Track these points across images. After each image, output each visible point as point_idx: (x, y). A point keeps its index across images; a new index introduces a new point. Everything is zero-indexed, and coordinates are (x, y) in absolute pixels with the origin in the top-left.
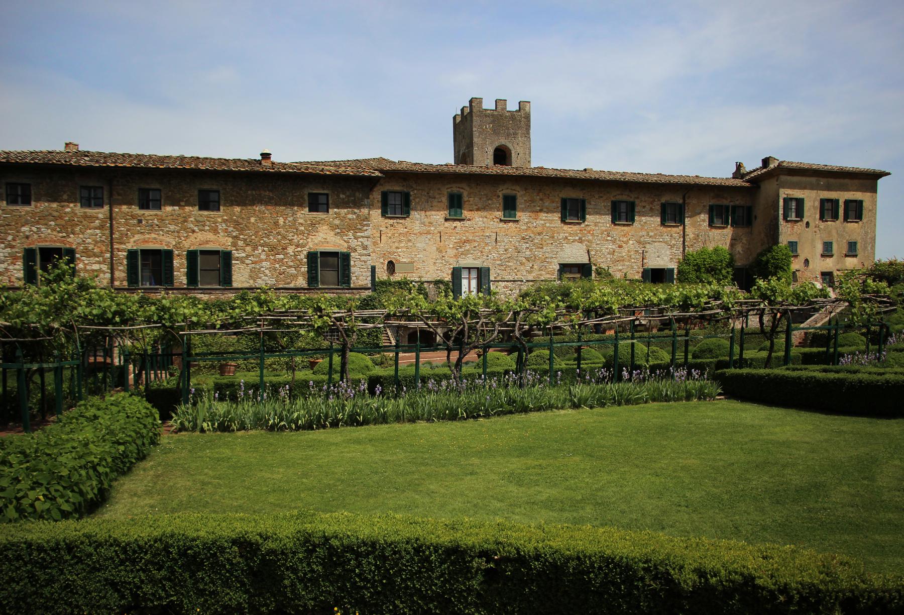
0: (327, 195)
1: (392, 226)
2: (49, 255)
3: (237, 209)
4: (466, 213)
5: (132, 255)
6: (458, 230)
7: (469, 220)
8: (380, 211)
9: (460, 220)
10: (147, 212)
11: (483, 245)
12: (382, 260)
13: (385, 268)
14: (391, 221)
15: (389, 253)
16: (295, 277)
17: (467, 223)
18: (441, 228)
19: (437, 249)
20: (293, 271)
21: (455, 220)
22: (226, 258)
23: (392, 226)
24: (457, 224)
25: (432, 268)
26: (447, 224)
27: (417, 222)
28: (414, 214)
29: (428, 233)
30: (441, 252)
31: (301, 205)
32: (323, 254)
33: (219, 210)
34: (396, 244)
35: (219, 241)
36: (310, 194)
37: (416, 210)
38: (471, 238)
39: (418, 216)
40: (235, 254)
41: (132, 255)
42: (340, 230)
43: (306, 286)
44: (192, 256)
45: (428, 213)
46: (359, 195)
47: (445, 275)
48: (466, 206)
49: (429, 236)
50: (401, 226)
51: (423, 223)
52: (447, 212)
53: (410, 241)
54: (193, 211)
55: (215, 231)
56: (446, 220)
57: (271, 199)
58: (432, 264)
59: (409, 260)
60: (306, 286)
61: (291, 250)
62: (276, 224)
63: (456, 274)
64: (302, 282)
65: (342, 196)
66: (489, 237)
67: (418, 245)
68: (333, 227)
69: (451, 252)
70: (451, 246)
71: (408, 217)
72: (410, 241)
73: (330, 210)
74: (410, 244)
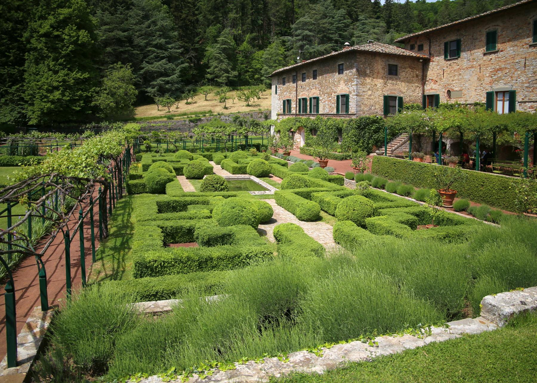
0: (343, 64)
1: (450, 65)
2: (288, 100)
3: (321, 77)
4: (499, 46)
5: (300, 100)
6: (492, 62)
7: (502, 51)
8: (443, 57)
9: (495, 53)
10: (304, 83)
11: (513, 70)
12: (444, 90)
13: (446, 95)
14: (449, 62)
15: (448, 85)
16: (333, 108)
17: (500, 54)
18: (481, 62)
19: (478, 78)
20: (333, 105)
21: (491, 53)
22: (317, 99)
23: (450, 65)
24: (493, 56)
25: (473, 93)
26: (485, 58)
27: (465, 60)
28: (463, 55)
29: (472, 67)
30: (480, 80)
31: (336, 72)
32: (342, 96)
33: (316, 79)
34: (452, 78)
35: (314, 93)
36: (339, 65)
37: (464, 51)
38: (503, 66)
39: (466, 56)
40: (321, 98)
41: (300, 100)
42: (347, 82)
43: (335, 113)
44: (311, 99)
45: (472, 52)
46: (353, 61)
47: (482, 99)
48: (500, 40)
49: (472, 69)
50: (455, 64)
51: (469, 60)
52: (485, 48)
53: (460, 74)
54: (311, 79)
55: (316, 88)
56: (485, 54)
57: (328, 70)
58: (474, 90)
59: (459, 89)
60: (335, 113)
61: (333, 95)
62: (329, 83)
63: (490, 96)
64: (335, 111)
65: (348, 63)
66: (518, 63)
67: (466, 77)
68: (345, 81)
69: (487, 80)
70: (488, 75)
71: (459, 57)
72: (460, 74)
73: (345, 72)
74: (460, 77)
